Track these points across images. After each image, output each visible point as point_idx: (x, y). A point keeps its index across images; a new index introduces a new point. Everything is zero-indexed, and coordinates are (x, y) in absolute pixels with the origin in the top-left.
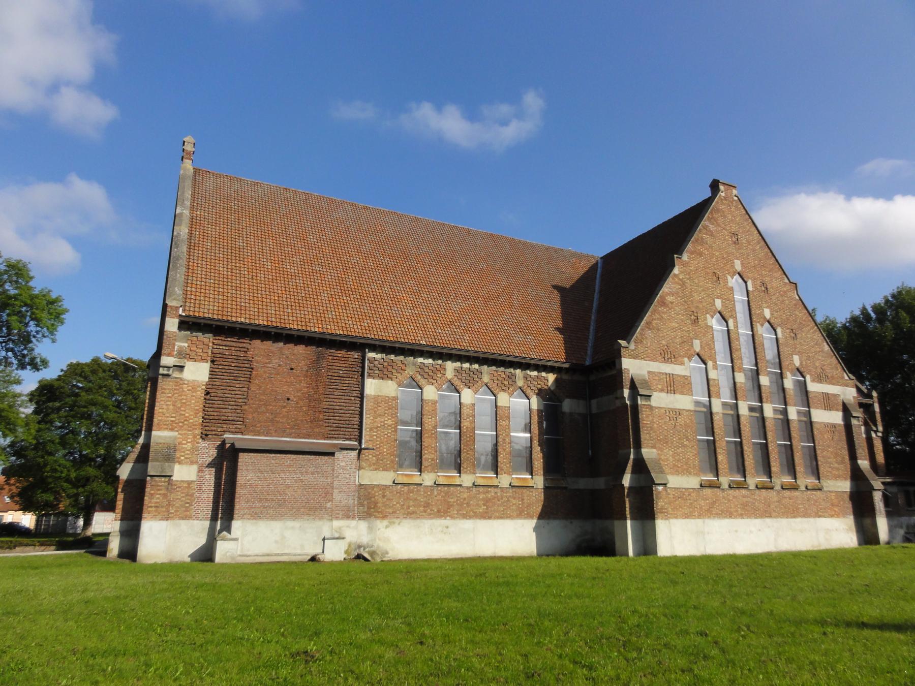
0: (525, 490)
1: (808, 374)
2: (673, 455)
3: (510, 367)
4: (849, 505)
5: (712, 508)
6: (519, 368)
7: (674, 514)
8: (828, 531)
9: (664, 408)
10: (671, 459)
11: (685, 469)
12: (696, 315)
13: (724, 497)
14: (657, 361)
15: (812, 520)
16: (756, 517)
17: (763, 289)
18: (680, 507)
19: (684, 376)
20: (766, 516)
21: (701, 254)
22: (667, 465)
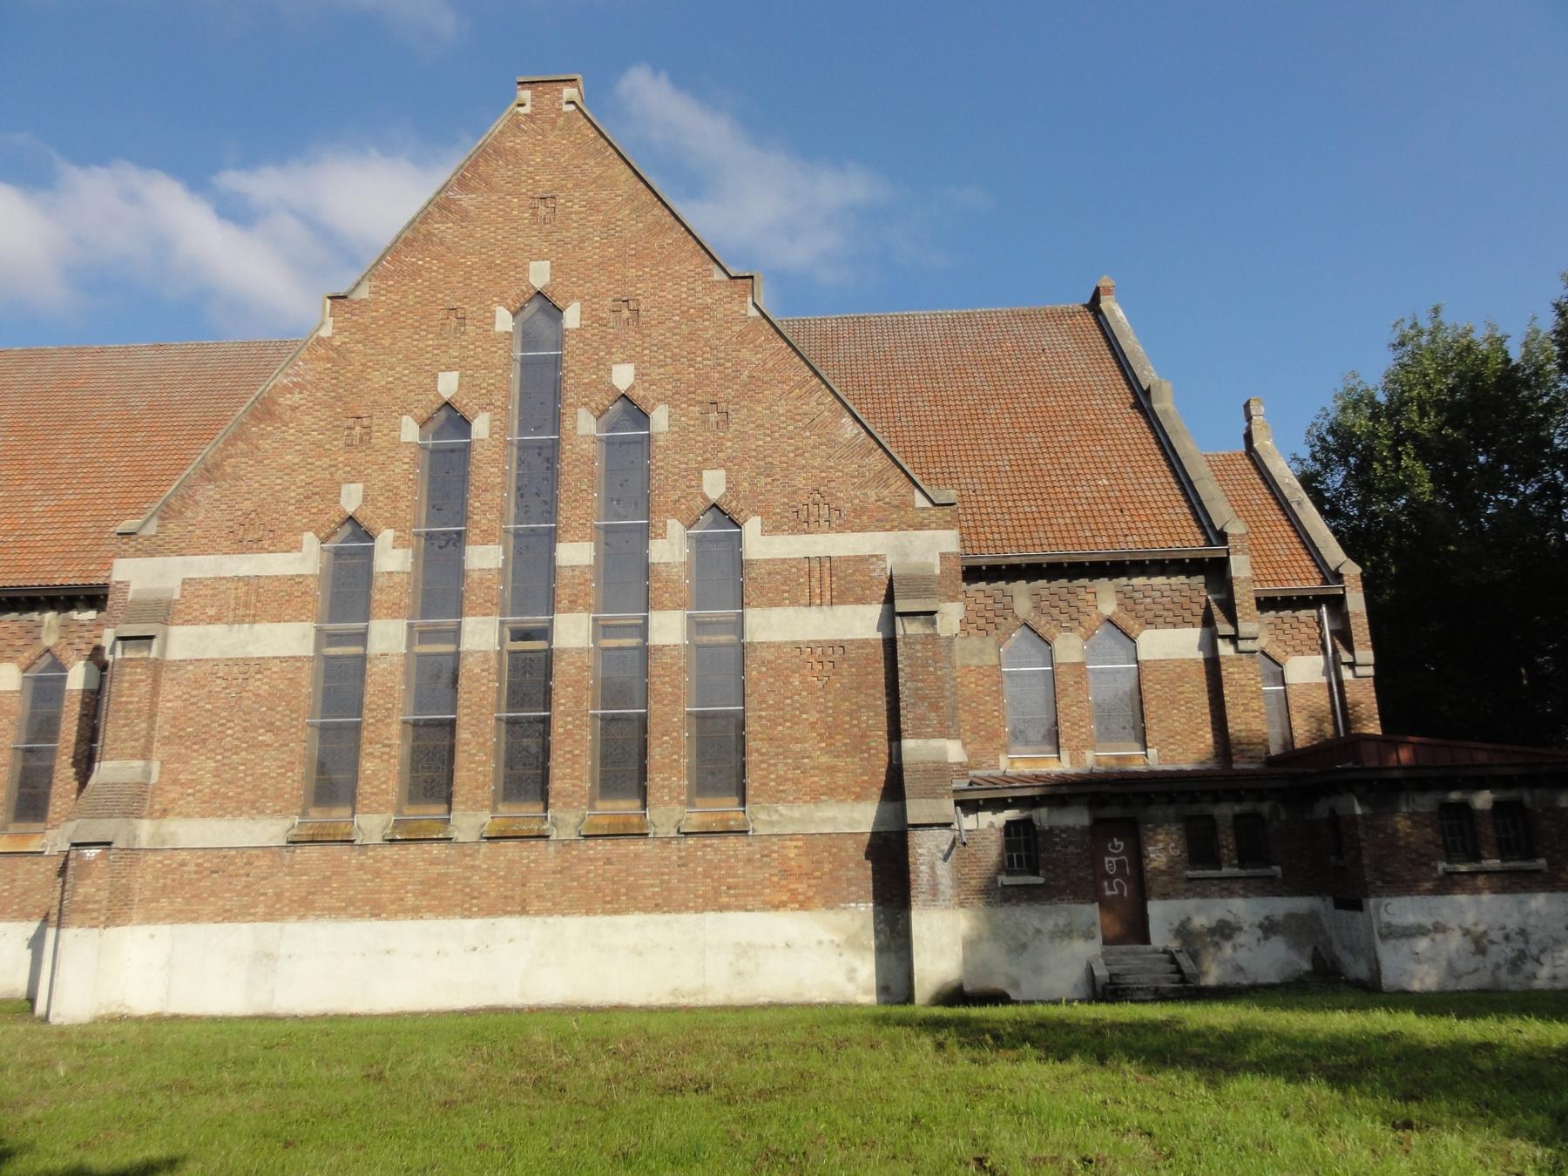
0: (24, 859)
1: (755, 513)
2: (217, 769)
3: (32, 609)
4: (864, 872)
5: (314, 893)
6: (53, 608)
7: (193, 911)
8: (744, 950)
9: (214, 660)
10: (208, 779)
11: (247, 801)
12: (365, 422)
13: (361, 867)
14: (215, 551)
15: (688, 919)
16: (467, 914)
17: (626, 314)
18: (213, 893)
19: (292, 578)
20: (506, 913)
21: (415, 273)
22: (193, 795)
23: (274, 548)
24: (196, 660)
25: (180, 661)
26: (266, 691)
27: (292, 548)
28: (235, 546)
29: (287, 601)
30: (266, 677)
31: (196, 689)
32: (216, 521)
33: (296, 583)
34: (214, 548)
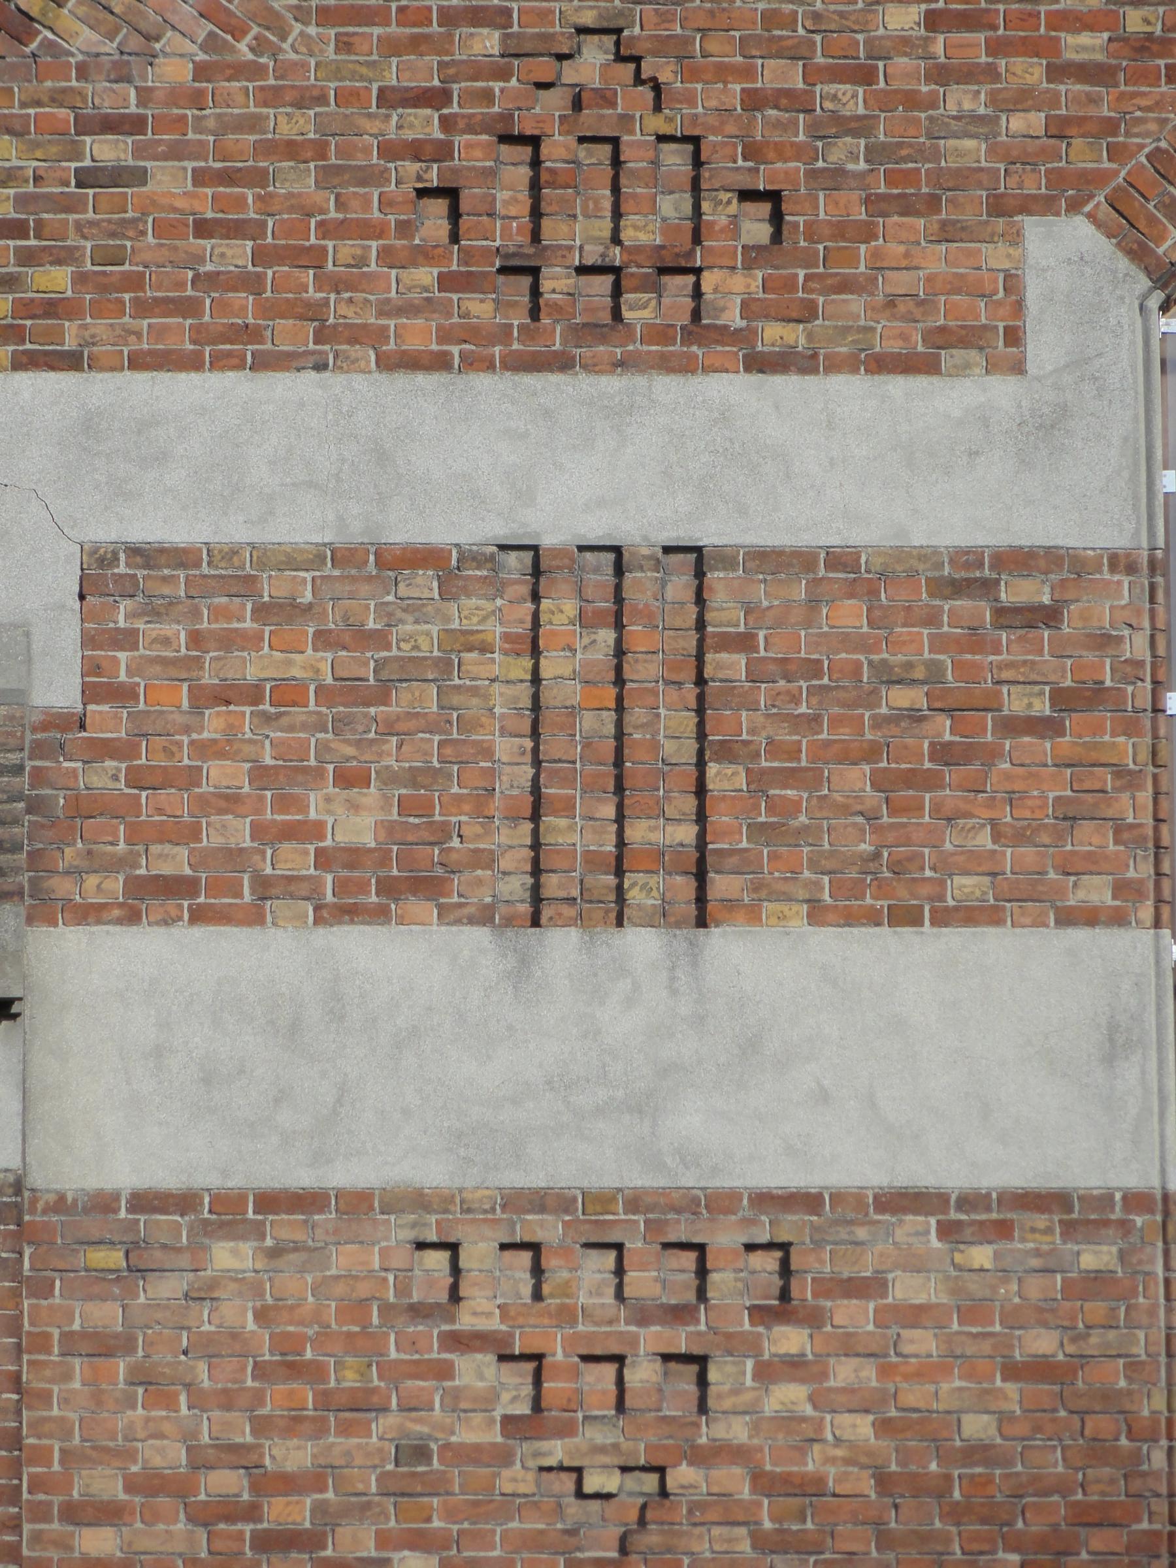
23: (795, 336)
24: (269, 1202)
25: (143, 1201)
26: (856, 1456)
27: (943, 338)
28: (480, 307)
29: (943, 753)
30: (849, 1347)
31: (294, 1424)
32: (306, 99)
33: (1005, 616)
34: (313, 313)
